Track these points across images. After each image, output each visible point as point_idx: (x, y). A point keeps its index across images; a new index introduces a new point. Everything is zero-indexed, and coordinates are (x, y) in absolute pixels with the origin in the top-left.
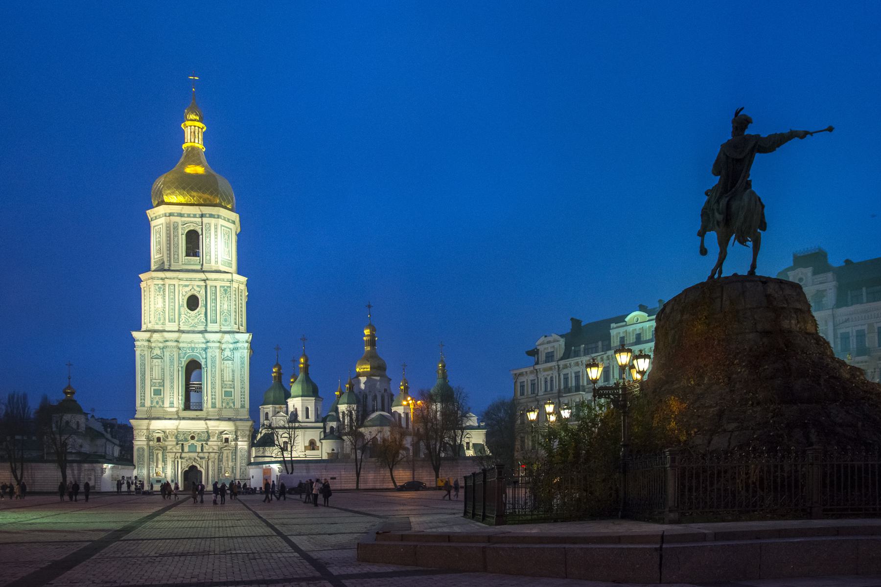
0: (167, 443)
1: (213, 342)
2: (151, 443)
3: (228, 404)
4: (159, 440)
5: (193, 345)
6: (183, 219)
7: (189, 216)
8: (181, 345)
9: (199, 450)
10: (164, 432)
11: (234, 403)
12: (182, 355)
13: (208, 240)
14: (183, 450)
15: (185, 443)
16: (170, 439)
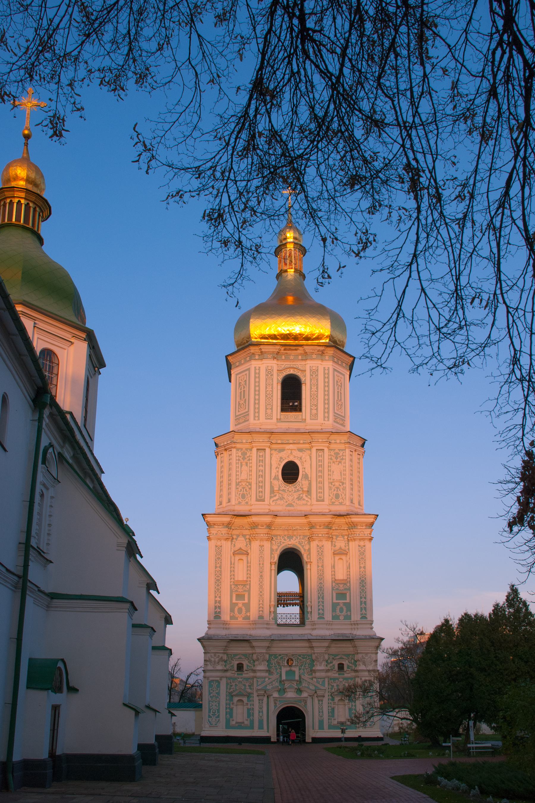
6: (279, 363)
13: (314, 389)
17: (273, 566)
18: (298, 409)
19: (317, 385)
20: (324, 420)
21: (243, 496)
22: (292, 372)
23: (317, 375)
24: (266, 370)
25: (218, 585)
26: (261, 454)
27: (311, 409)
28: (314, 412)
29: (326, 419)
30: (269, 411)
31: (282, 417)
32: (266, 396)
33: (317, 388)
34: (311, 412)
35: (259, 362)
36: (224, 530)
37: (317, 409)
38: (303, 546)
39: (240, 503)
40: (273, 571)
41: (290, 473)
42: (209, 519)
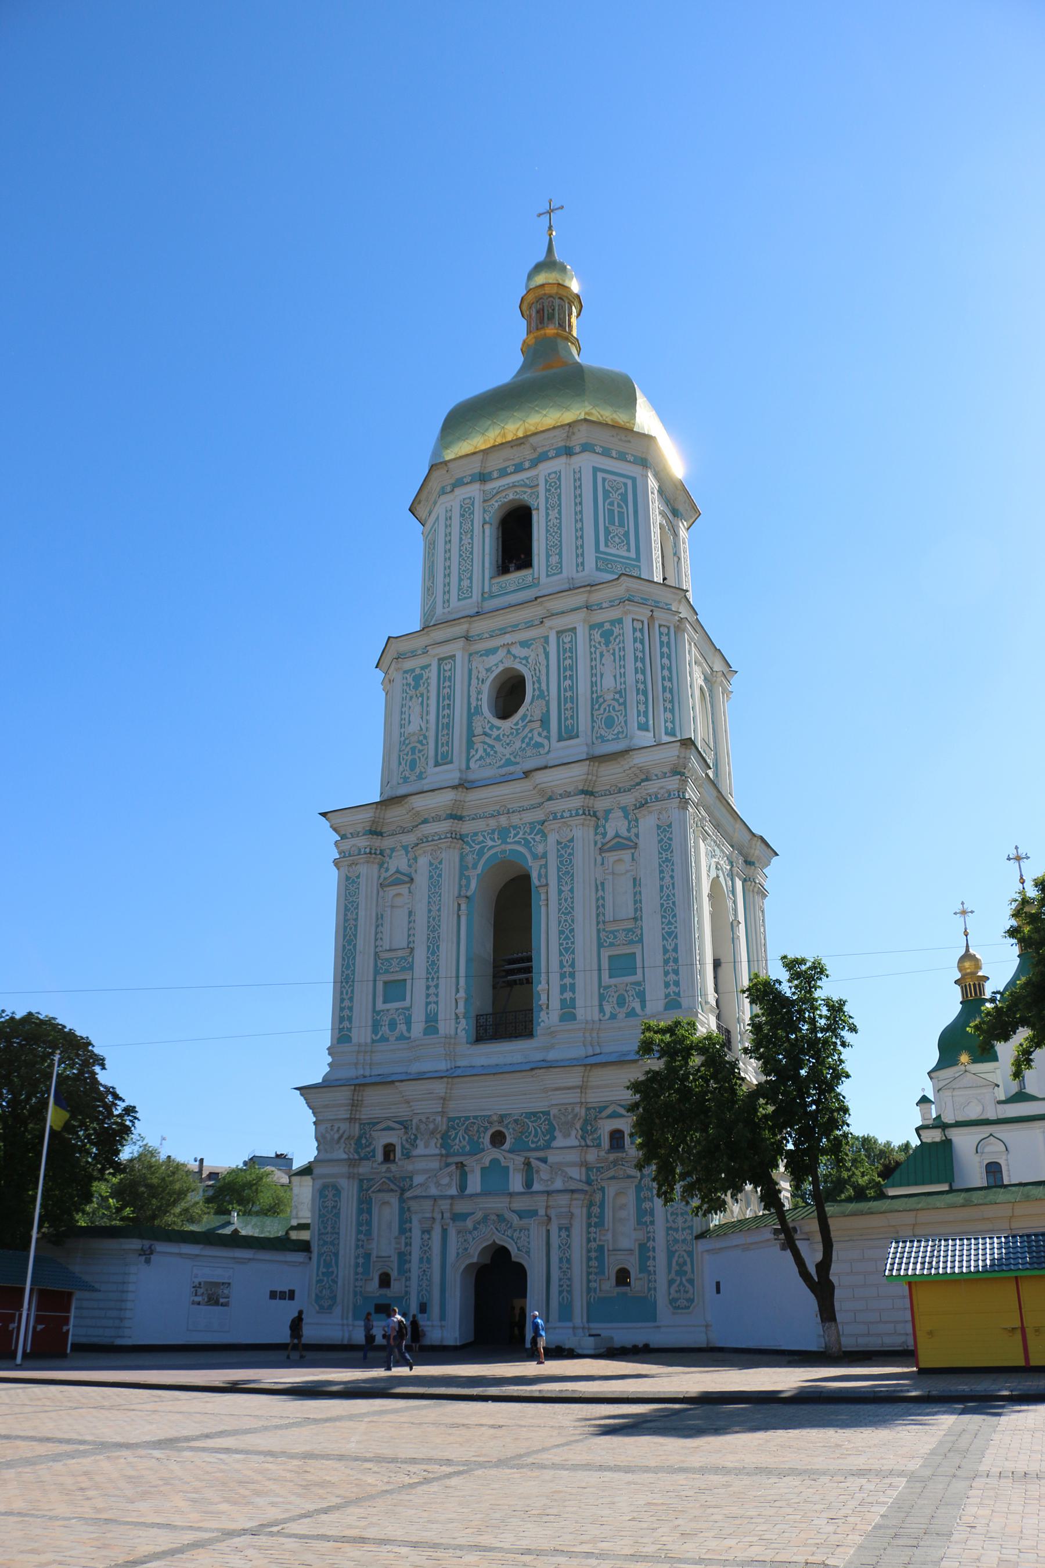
0: (409, 1166)
1: (568, 795)
2: (364, 1169)
3: (621, 1002)
4: (389, 1151)
5: (503, 821)
6: (490, 486)
7: (503, 473)
8: (467, 827)
9: (516, 1183)
10: (405, 1125)
11: (642, 996)
12: (470, 858)
13: (554, 514)
14: (463, 1187)
15: (468, 1161)
16: (420, 1150)
17: (463, 907)
18: (527, 563)
19: (560, 505)
20: (577, 571)
21: (413, 765)
22: (511, 497)
23: (560, 487)
24: (461, 506)
25: (348, 968)
26: (447, 667)
27: (548, 556)
28: (554, 559)
29: (580, 568)
30: (466, 583)
31: (494, 589)
32: (461, 556)
33: (560, 513)
34: (548, 561)
35: (450, 497)
36: (362, 842)
37: (560, 554)
38: (530, 849)
39: (406, 780)
40: (463, 919)
41: (510, 694)
42: (333, 822)
